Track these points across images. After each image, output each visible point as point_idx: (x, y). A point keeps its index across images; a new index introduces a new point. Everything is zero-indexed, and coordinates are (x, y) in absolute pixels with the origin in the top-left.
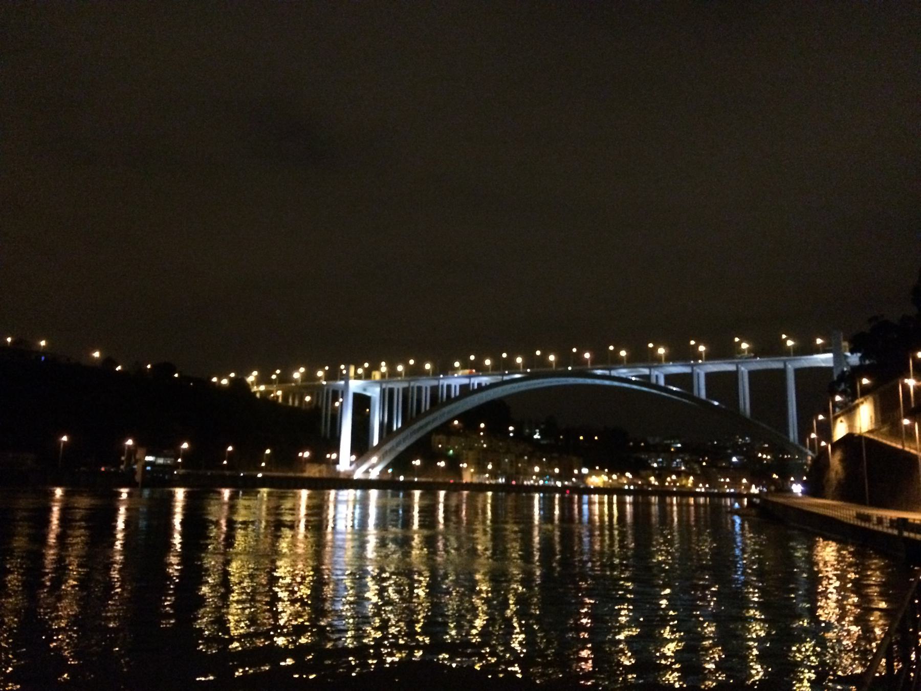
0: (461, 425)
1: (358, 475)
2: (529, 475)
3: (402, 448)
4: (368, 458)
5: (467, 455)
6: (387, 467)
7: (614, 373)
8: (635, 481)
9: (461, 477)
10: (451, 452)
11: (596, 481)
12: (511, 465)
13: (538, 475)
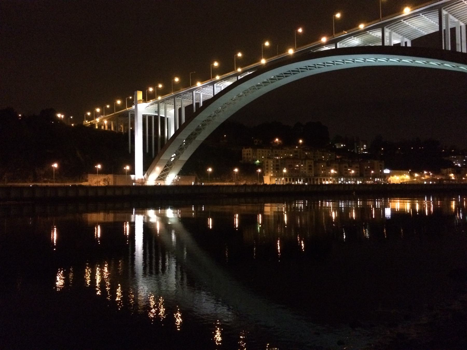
0: (280, 141)
1: (152, 180)
2: (327, 176)
3: (185, 157)
4: (153, 169)
5: (267, 162)
6: (178, 175)
7: (339, 45)
8: (435, 178)
9: (262, 180)
10: (258, 161)
11: (396, 179)
12: (310, 169)
13: (334, 176)
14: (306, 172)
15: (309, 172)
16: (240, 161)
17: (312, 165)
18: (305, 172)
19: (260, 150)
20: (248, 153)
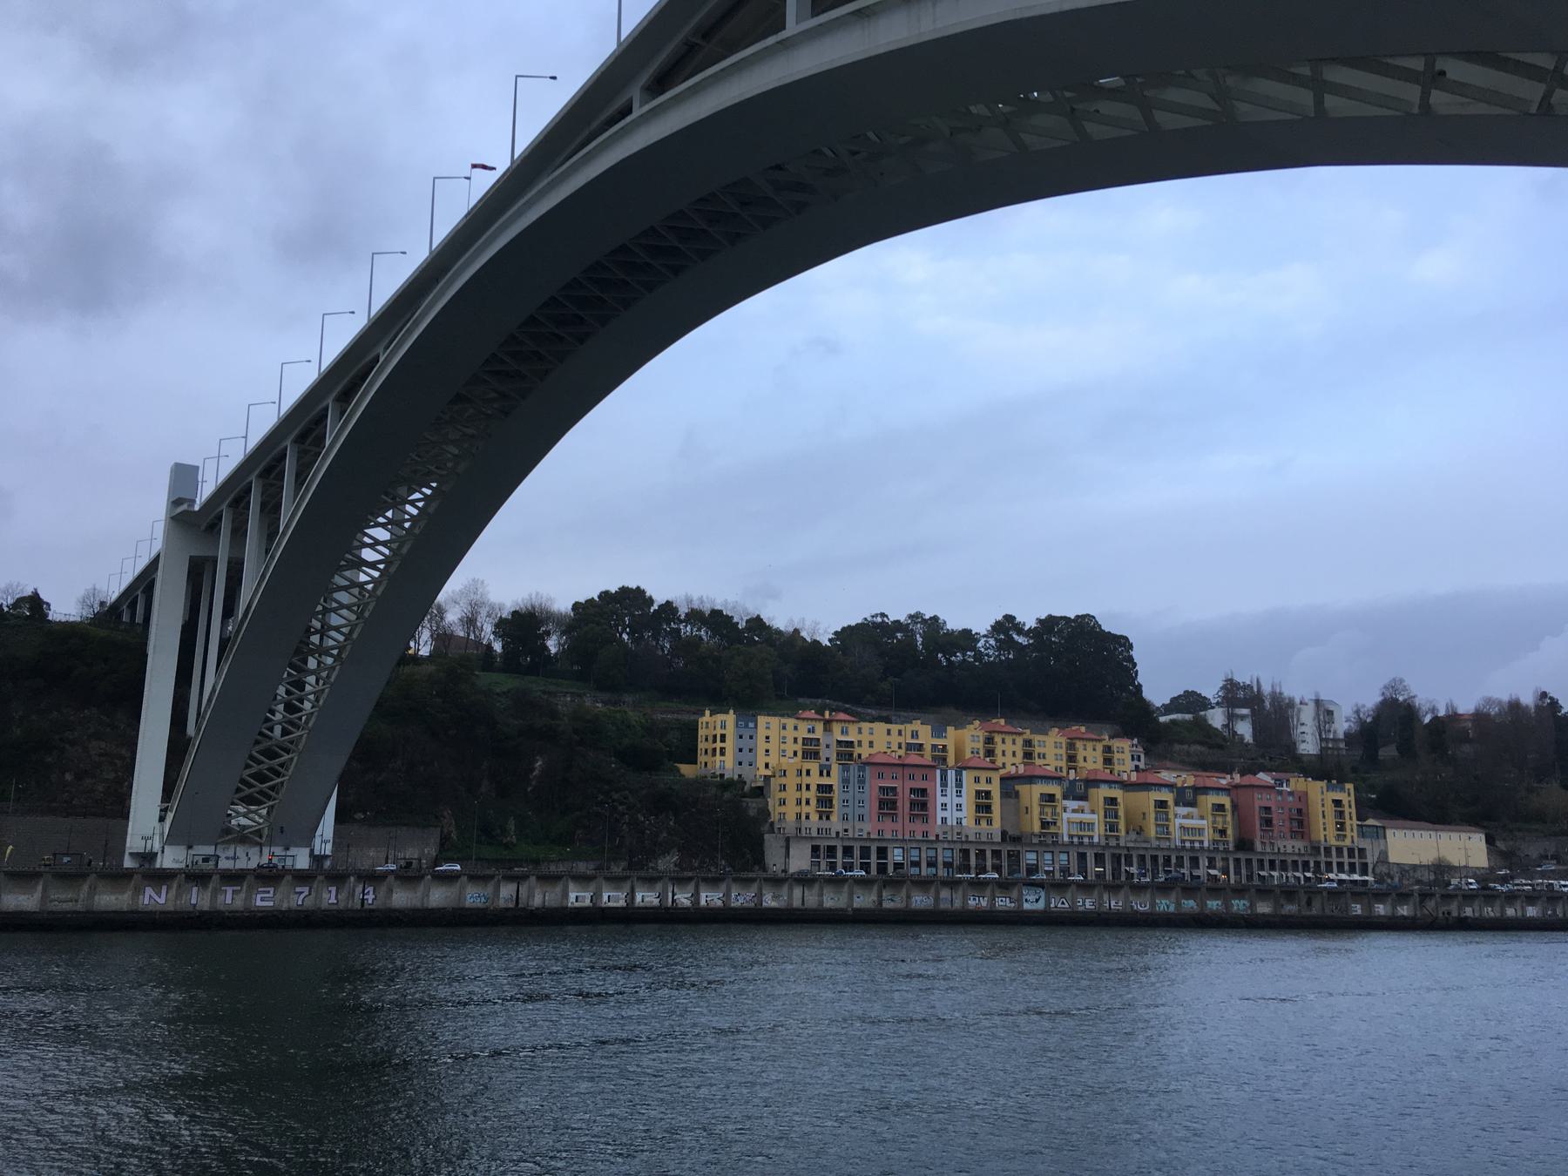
14: (964, 822)
15: (978, 821)
16: (686, 769)
17: (995, 789)
18: (959, 822)
19: (775, 721)
20: (719, 732)
